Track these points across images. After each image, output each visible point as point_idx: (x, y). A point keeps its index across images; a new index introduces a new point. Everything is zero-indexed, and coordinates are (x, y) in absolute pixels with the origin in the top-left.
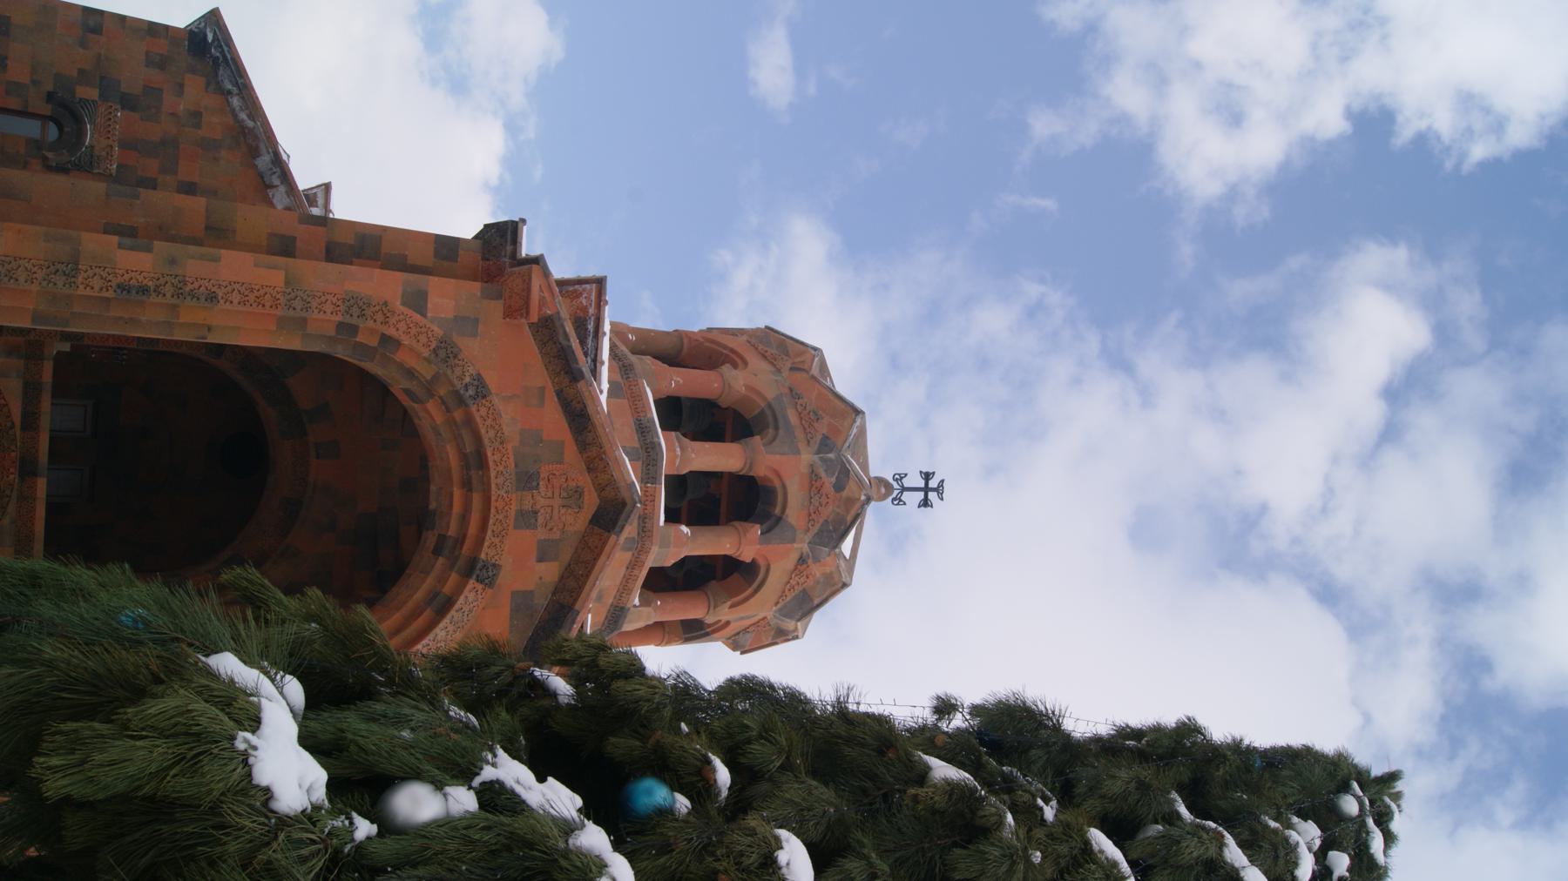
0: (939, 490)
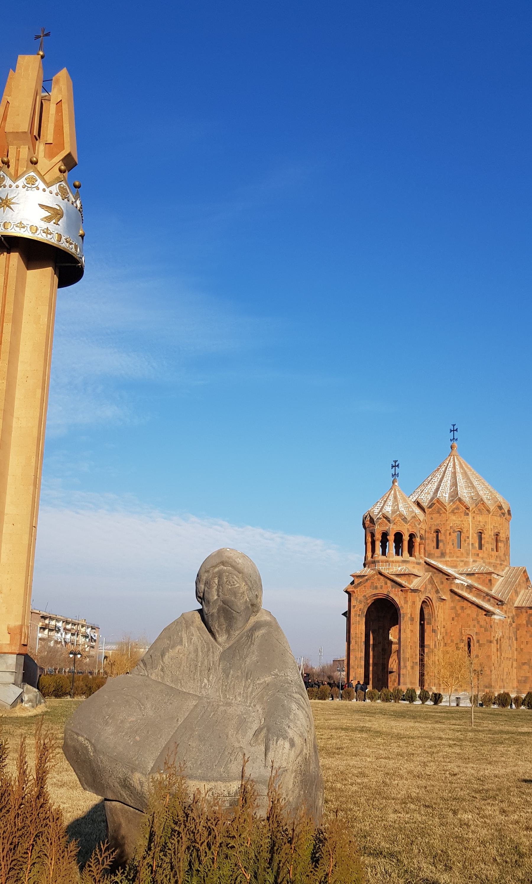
0: (395, 462)
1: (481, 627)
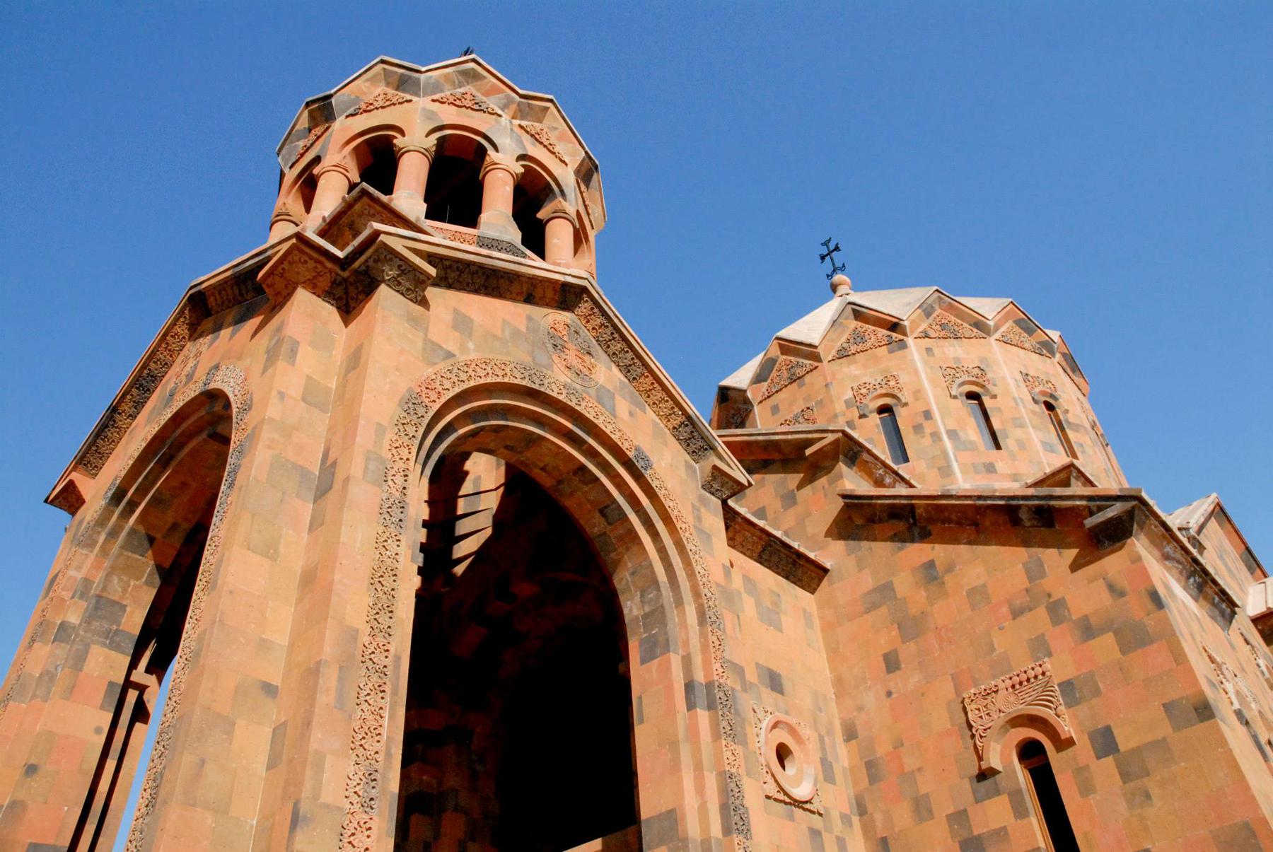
1: (1088, 630)
